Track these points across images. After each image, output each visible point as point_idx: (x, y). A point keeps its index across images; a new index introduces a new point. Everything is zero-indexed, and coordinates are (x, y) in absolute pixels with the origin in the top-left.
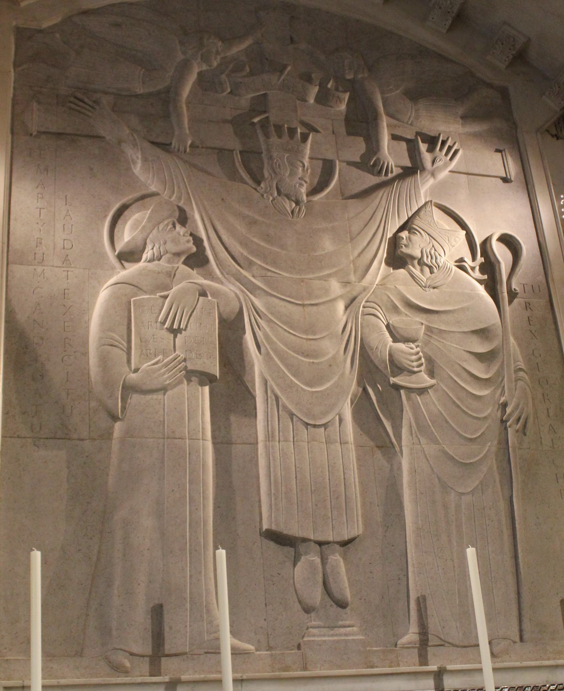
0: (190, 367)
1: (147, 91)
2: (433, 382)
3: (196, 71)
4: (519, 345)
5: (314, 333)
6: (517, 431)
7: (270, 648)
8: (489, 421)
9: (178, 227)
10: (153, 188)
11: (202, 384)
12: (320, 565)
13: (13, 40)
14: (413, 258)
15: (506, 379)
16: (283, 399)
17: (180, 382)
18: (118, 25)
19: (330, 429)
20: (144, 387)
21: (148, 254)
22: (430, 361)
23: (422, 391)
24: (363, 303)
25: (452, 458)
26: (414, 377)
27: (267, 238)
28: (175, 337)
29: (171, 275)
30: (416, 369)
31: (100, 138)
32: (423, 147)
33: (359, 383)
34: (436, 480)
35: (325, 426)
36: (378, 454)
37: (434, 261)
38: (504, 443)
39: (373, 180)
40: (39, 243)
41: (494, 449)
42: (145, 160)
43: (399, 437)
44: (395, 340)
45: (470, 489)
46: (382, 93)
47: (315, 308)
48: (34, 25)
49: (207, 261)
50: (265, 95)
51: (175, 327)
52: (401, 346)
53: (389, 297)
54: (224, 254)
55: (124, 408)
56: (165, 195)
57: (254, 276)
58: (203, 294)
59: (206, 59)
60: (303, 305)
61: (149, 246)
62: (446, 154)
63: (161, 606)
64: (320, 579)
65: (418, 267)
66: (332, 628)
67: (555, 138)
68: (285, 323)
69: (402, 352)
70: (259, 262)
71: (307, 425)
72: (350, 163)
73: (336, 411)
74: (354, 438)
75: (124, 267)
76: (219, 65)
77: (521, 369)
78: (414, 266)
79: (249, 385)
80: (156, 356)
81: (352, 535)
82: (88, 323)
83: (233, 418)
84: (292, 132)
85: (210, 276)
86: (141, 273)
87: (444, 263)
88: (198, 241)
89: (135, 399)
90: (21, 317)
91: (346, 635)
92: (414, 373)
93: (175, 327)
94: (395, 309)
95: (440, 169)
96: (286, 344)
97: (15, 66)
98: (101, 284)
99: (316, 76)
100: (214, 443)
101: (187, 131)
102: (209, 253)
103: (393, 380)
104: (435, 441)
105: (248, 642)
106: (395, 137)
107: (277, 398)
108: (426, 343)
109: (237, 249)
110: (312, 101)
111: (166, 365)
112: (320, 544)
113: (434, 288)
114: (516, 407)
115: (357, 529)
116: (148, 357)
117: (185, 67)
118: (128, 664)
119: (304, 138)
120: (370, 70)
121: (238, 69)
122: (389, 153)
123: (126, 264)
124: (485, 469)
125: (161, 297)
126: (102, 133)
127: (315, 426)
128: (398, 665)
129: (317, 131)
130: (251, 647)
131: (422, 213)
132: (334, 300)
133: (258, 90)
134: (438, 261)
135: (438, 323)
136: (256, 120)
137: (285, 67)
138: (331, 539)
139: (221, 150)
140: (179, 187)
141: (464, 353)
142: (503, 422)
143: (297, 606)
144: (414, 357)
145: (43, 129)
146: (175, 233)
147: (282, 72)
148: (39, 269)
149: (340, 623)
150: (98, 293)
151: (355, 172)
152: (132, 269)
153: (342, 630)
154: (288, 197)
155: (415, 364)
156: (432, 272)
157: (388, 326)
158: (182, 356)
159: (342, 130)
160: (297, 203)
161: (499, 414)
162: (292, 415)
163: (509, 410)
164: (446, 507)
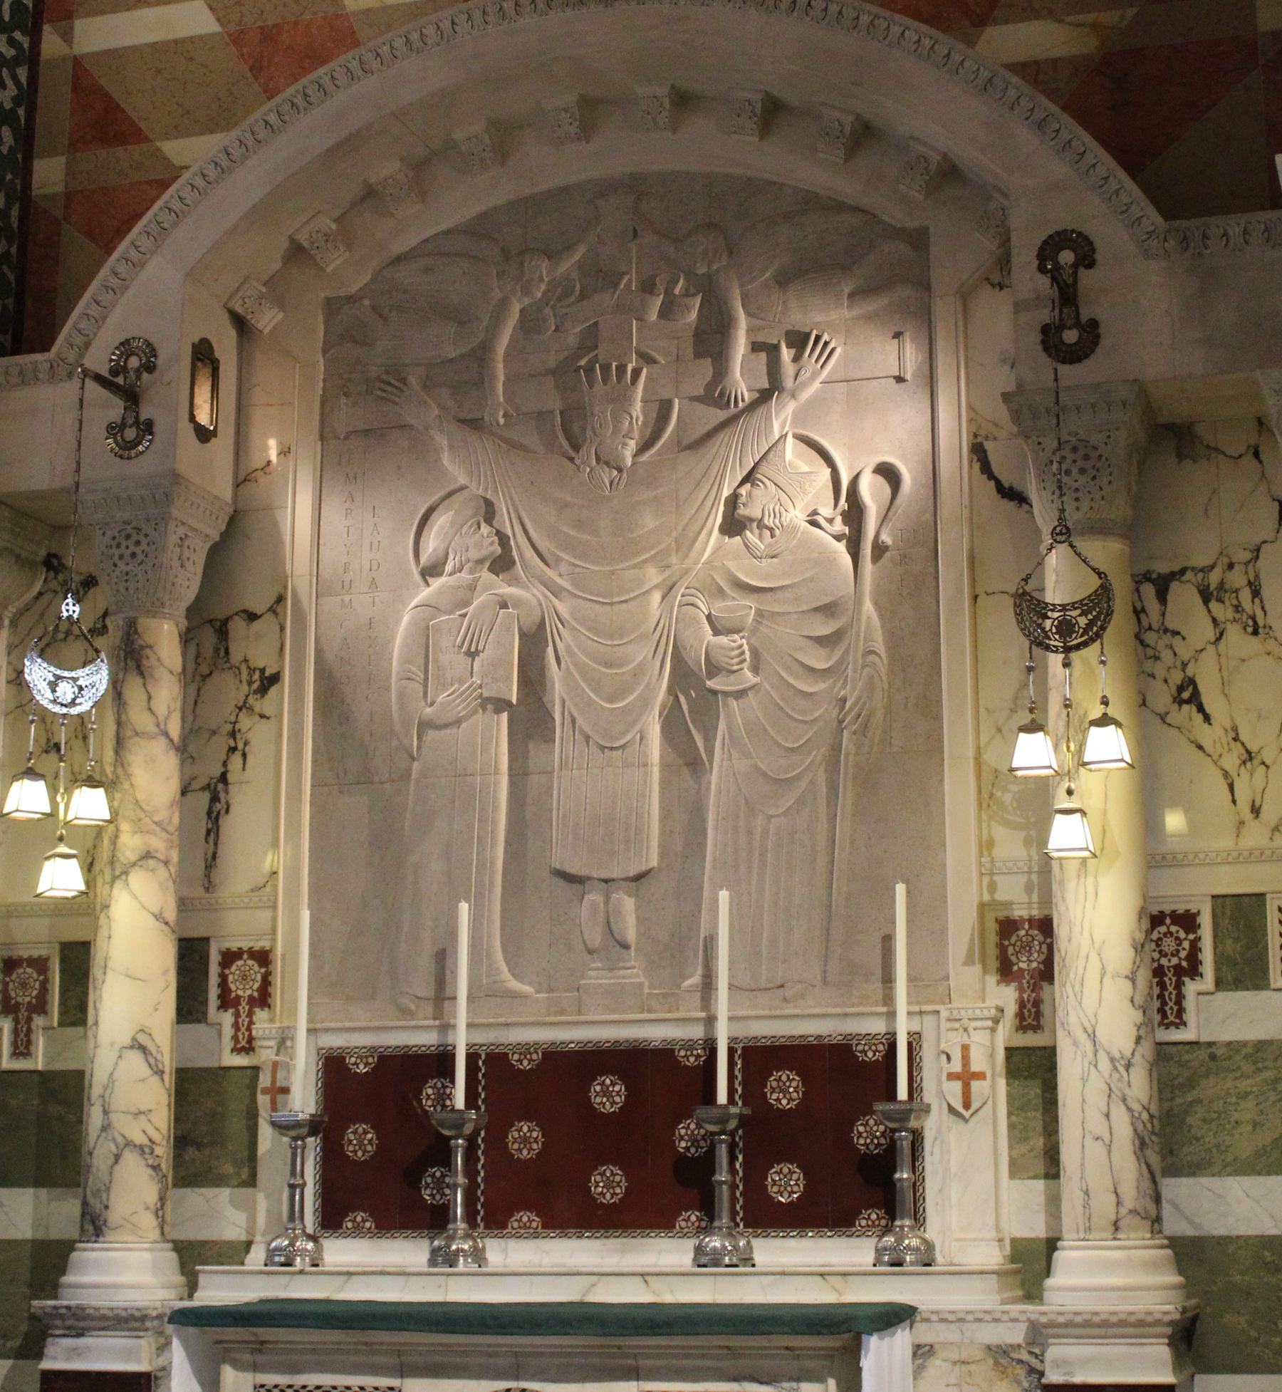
0: (486, 694)
1: (458, 352)
2: (757, 679)
3: (515, 309)
4: (881, 616)
5: (621, 637)
6: (854, 733)
7: (550, 990)
8: (820, 724)
9: (483, 525)
10: (462, 480)
11: (498, 711)
12: (602, 905)
13: (321, 318)
14: (751, 520)
15: (850, 667)
16: (580, 722)
17: (474, 712)
18: (428, 270)
19: (629, 750)
20: (438, 722)
21: (449, 567)
22: (755, 653)
23: (740, 694)
24: (683, 590)
25: (765, 774)
26: (732, 677)
27: (579, 524)
28: (473, 660)
29: (472, 588)
30: (735, 668)
31: (411, 426)
32: (786, 354)
33: (670, 690)
34: (743, 802)
35: (623, 747)
36: (686, 772)
37: (777, 521)
38: (836, 748)
39: (722, 415)
40: (346, 568)
41: (819, 758)
42: (451, 447)
43: (710, 751)
44: (716, 632)
45: (781, 810)
46: (741, 286)
47: (624, 605)
49: (514, 563)
50: (596, 323)
51: (473, 649)
52: (723, 640)
53: (713, 579)
54: (529, 553)
55: (419, 747)
56: (473, 486)
57: (560, 575)
58: (504, 605)
59: (526, 292)
60: (612, 604)
61: (451, 556)
62: (817, 361)
63: (444, 950)
64: (601, 917)
65: (757, 531)
66: (612, 970)
67: (998, 288)
68: (589, 629)
69: (722, 647)
70: (566, 557)
71: (603, 748)
72: (693, 399)
73: (637, 728)
74: (661, 756)
75: (428, 584)
76: (545, 293)
77: (871, 652)
78: (752, 532)
79: (548, 706)
80: (452, 685)
81: (644, 868)
82: (391, 654)
83: (531, 746)
84: (621, 369)
85: (515, 582)
86: (440, 591)
87: (791, 521)
88: (503, 539)
89: (431, 735)
90: (329, 656)
91: (624, 977)
92: (734, 672)
93: (473, 649)
94: (721, 593)
95: (804, 385)
96: (588, 656)
97: (325, 352)
98: (405, 606)
100: (510, 776)
101: (502, 399)
102: (515, 553)
103: (709, 683)
104: (747, 755)
105: (530, 984)
106: (756, 347)
107: (573, 721)
108: (754, 631)
109: (543, 545)
110: (653, 316)
111: (461, 694)
112: (606, 881)
113: (772, 557)
114: (854, 705)
115: (654, 861)
116: (444, 687)
117: (504, 304)
118: (413, 1007)
119: (636, 373)
120: (731, 253)
121: (567, 293)
122: (742, 375)
123: (430, 580)
124: (803, 784)
125: (461, 616)
126: (410, 421)
127: (612, 749)
128: (678, 1009)
129: (654, 362)
130: (529, 989)
131: (771, 455)
132: (648, 592)
133: (586, 320)
134: (783, 519)
135: (770, 604)
136: (583, 363)
138: (615, 876)
139: (540, 414)
140: (486, 476)
141: (800, 638)
142: (840, 722)
143: (582, 947)
144: (736, 652)
145: (351, 429)
146: (477, 536)
147: (616, 285)
148: (347, 599)
149: (621, 964)
150: (401, 617)
151: (701, 408)
152: (437, 583)
153: (622, 972)
154: (607, 464)
155: (736, 660)
156: (772, 536)
157: (709, 617)
158: (479, 682)
159: (690, 351)
160: (620, 470)
161: (835, 712)
162: (587, 738)
163: (848, 705)
164: (750, 833)
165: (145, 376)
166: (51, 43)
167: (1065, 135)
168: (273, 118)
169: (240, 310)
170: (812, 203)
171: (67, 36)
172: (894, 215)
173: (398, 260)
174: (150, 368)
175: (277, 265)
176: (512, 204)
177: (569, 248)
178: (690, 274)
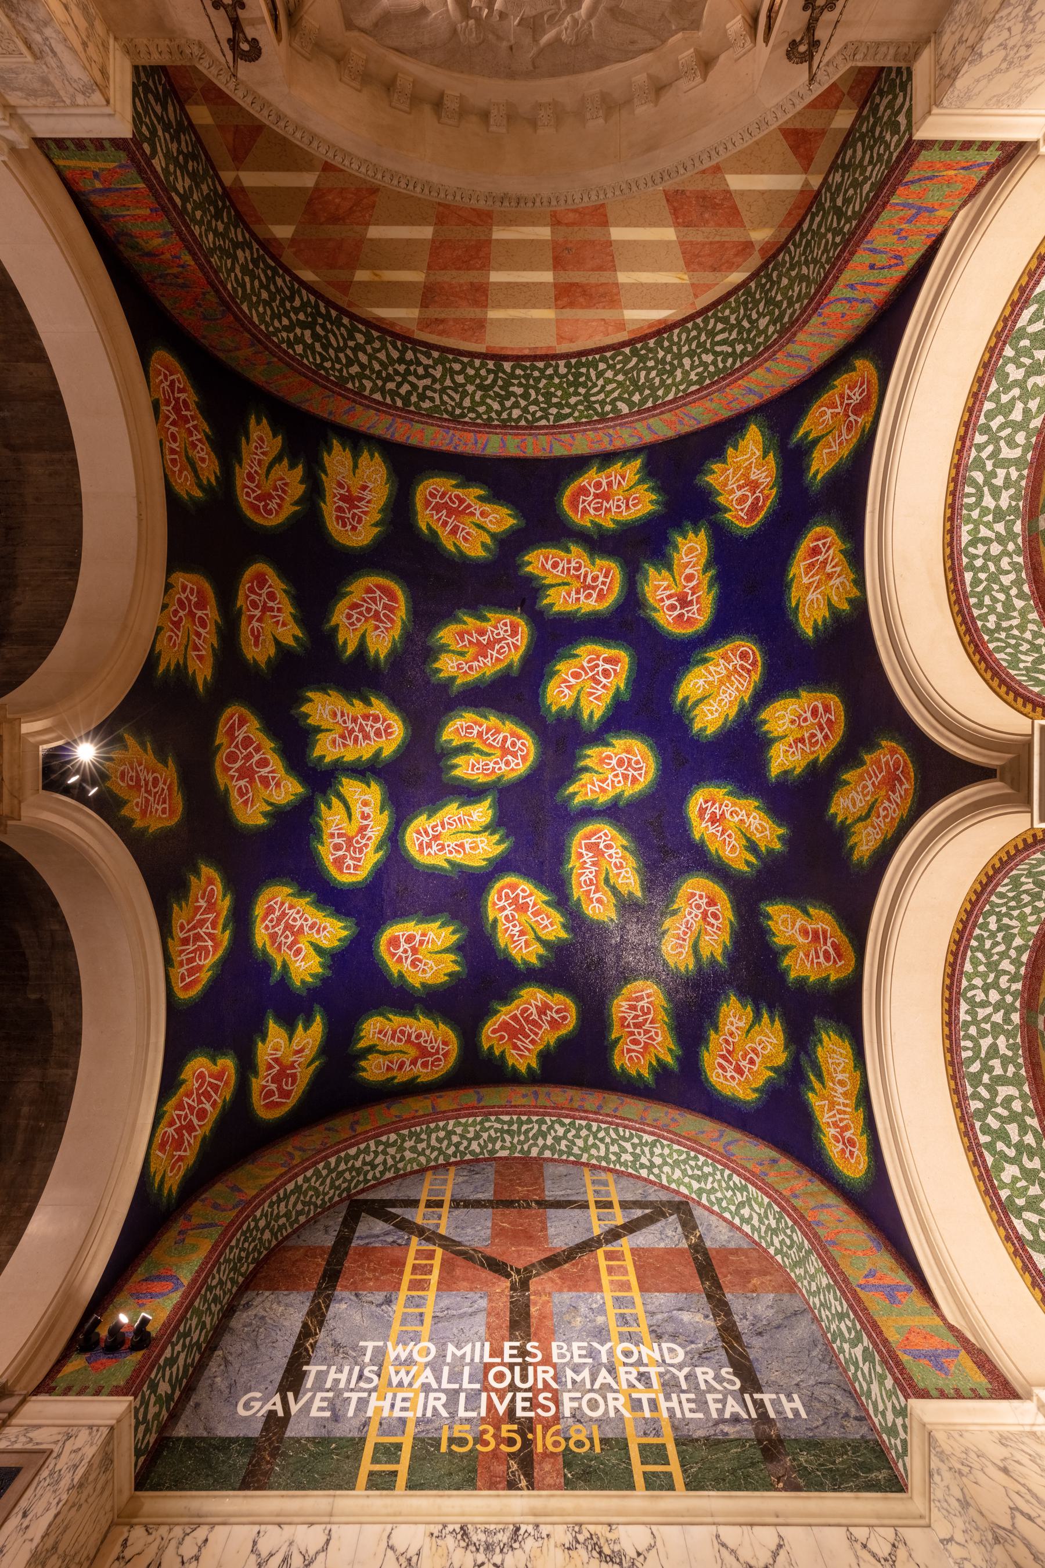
18: (633, 42)
48: (688, 34)
59: (575, 21)
99: (496, 17)
117: (592, 12)
137: (519, 24)
147: (522, 19)
165: (798, 39)
166: (816, 182)
167: (265, 112)
168: (682, 171)
169: (748, 39)
170: (414, 53)
171: (807, 183)
172: (366, 41)
173: (651, 50)
174: (794, 44)
175: (722, 58)
176: (582, 71)
177: (550, 44)
178: (478, 19)
